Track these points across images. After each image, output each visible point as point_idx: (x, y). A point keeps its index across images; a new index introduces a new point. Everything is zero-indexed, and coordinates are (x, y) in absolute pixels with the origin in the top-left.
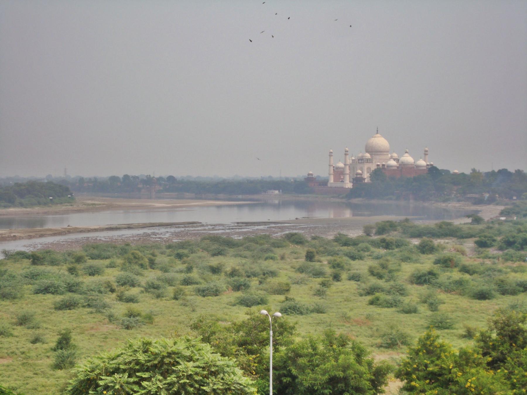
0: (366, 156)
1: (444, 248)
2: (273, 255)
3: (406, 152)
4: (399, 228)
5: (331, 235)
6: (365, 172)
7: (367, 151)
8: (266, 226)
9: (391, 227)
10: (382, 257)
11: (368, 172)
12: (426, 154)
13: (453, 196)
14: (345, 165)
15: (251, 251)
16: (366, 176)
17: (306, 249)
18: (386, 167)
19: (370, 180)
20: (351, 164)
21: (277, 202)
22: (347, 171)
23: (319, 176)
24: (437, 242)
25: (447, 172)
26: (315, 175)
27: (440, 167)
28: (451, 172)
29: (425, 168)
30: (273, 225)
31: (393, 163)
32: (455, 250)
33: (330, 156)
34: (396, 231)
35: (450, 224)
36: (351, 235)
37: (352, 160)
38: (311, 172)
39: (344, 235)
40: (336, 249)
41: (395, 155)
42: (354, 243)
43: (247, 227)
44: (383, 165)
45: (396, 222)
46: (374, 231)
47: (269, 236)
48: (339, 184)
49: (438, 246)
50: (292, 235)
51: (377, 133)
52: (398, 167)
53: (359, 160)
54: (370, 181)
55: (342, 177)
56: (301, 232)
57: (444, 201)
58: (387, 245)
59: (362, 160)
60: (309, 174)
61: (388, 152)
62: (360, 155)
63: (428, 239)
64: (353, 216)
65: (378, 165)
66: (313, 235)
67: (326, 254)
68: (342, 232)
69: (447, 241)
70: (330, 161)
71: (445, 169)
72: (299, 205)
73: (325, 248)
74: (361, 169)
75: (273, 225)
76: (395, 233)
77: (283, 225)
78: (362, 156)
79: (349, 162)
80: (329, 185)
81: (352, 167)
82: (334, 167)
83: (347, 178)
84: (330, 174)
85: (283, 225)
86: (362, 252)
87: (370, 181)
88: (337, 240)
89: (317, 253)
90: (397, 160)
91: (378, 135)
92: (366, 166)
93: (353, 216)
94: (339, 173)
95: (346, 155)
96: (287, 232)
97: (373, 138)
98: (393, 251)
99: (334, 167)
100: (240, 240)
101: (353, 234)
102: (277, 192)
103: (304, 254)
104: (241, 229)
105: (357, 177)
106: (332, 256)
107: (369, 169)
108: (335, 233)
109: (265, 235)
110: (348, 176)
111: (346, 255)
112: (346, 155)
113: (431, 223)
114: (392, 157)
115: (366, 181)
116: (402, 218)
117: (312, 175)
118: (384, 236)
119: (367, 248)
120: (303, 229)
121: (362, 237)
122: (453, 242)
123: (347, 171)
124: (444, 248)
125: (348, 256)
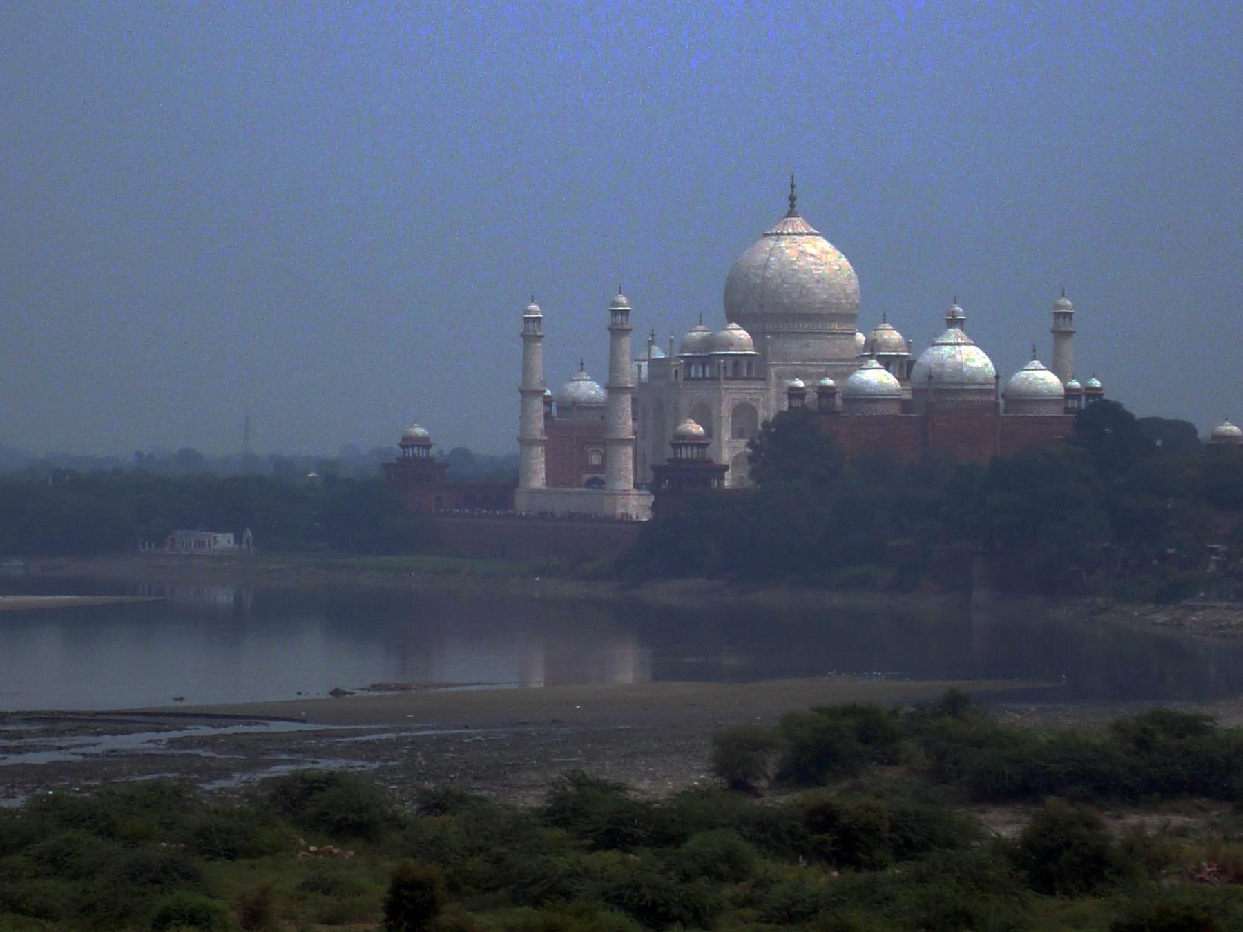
0: (729, 344)
1: (1159, 864)
2: (202, 899)
3: (953, 322)
4: (910, 745)
5: (534, 786)
6: (726, 435)
7: (735, 315)
8: (164, 736)
9: (866, 740)
10: (815, 911)
11: (738, 433)
12: (1061, 335)
13: (1213, 567)
14: (614, 389)
15: (75, 877)
16: (729, 450)
17: (389, 865)
18: (839, 401)
19: (752, 474)
20: (641, 384)
21: (224, 597)
22: (626, 426)
23: (461, 454)
24: (1121, 825)
25: (1182, 431)
26: (442, 447)
27: (1139, 408)
28: (1203, 433)
29: (1056, 411)
30: (206, 731)
31: (876, 377)
32: (1222, 870)
33: (529, 338)
34: (893, 763)
35: (1193, 726)
36: (645, 785)
37: (653, 363)
38: (420, 431)
39: (605, 787)
40: (561, 864)
41: (892, 335)
42: (661, 830)
43: (66, 741)
44: (825, 392)
45: (894, 713)
46: (772, 763)
47: (178, 793)
48: (575, 499)
49: (1130, 850)
50: (314, 785)
51: (791, 213)
52: (905, 405)
53: (689, 362)
54: (749, 483)
55: (595, 460)
56: (358, 766)
57: (1169, 595)
58: (843, 841)
59: (706, 364)
60: (409, 442)
61: (849, 317)
62: (697, 334)
63: (1072, 810)
64: (656, 677)
65: (795, 393)
66: (430, 785)
67: (501, 892)
68: (590, 771)
69: (1177, 820)
70: (526, 369)
71: (1169, 414)
72: (352, 617)
73: (499, 860)
74: (704, 415)
75: (206, 731)
76: (892, 774)
77: (255, 729)
78: (709, 343)
79: (634, 371)
80: (521, 504)
81: (655, 402)
82: (548, 401)
83: (625, 460)
84: (526, 442)
85: (255, 729)
86: (703, 882)
87: (749, 483)
88: (564, 813)
89: (453, 887)
90: (900, 365)
91: (799, 224)
92: (730, 395)
93: (656, 677)
94: (577, 436)
95: (617, 332)
96: (283, 770)
97: (771, 242)
98: (880, 875)
99: (548, 401)
100: (11, 812)
101: (654, 784)
102: (224, 540)
103: (379, 891)
104: (19, 750)
105: (676, 461)
106: (537, 903)
107: (743, 411)
108: (555, 775)
109: (157, 787)
110: (629, 450)
111: (616, 898)
112: (617, 332)
113: (1092, 723)
114: (873, 350)
115: (726, 484)
116: (934, 688)
117: (424, 443)
118: (828, 794)
119: (730, 857)
120: (372, 751)
121: (703, 794)
122: (1213, 825)
123: (626, 426)
124: (1159, 864)
125: (627, 908)
